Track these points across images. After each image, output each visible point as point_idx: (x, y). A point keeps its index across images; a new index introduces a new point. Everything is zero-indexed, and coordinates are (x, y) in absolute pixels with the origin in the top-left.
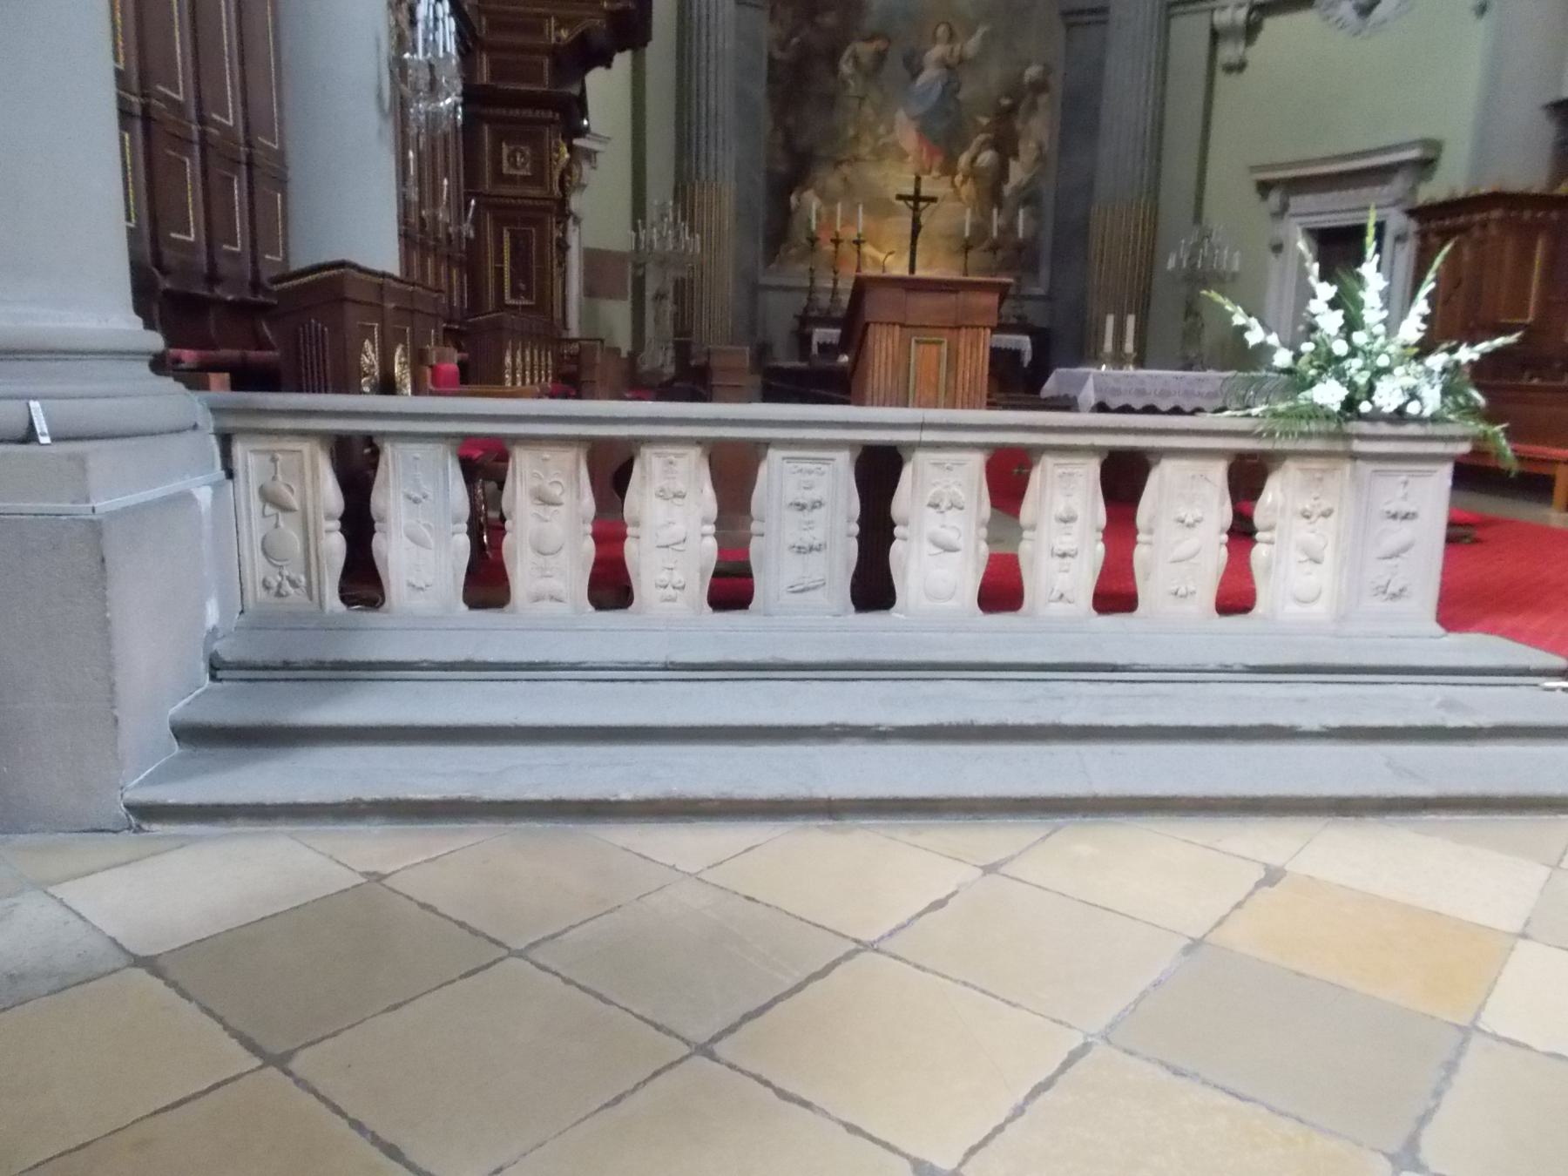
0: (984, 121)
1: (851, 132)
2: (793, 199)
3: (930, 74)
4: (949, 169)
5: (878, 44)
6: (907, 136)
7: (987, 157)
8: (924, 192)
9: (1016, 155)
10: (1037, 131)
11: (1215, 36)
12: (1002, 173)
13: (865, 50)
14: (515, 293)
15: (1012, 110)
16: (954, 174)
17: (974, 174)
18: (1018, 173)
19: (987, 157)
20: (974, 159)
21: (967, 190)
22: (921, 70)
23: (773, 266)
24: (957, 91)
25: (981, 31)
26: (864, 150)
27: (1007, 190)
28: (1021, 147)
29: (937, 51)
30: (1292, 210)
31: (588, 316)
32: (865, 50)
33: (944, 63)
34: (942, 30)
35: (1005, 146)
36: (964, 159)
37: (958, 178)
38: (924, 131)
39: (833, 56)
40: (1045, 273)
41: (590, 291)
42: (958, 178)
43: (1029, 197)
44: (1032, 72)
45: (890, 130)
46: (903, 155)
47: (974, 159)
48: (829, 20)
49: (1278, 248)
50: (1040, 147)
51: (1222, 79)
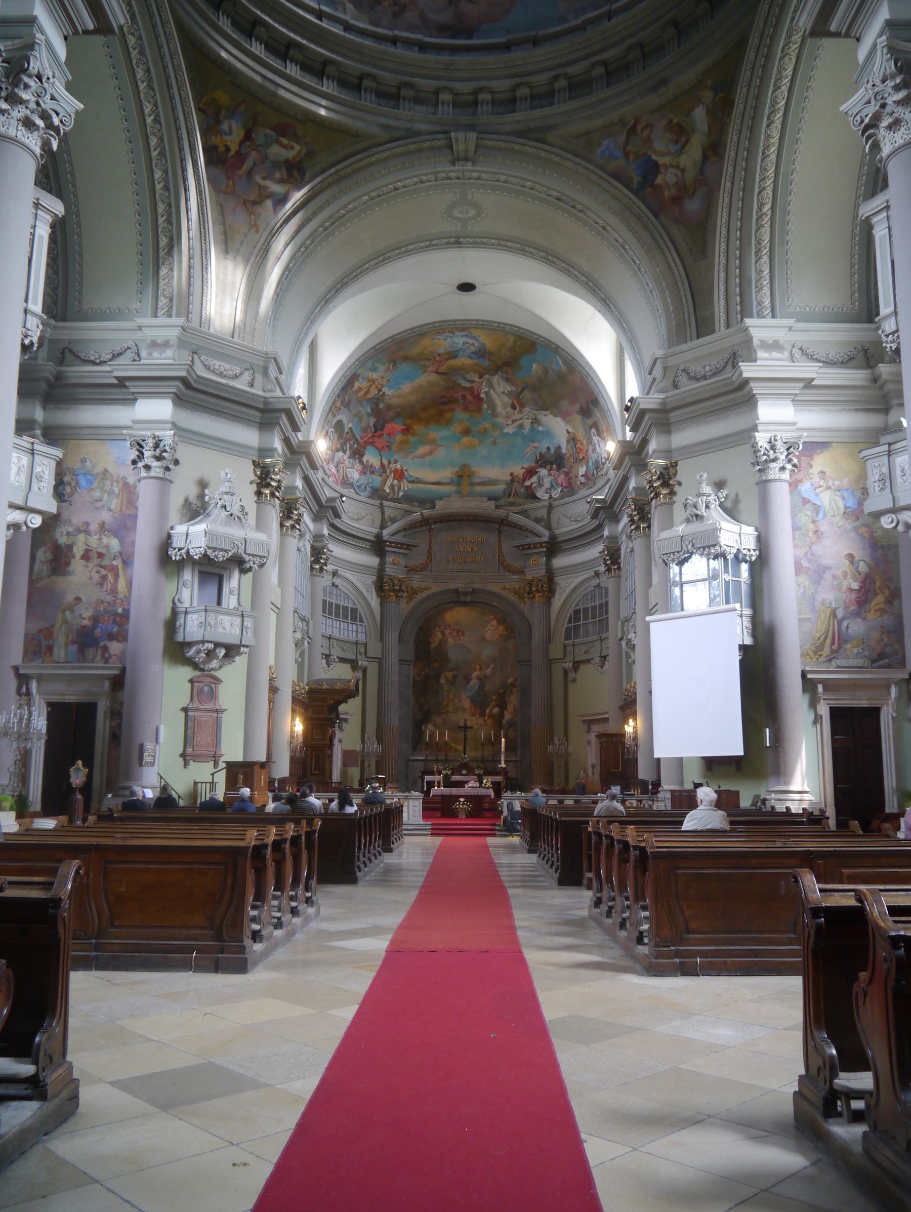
0: (494, 697)
1: (445, 702)
2: (423, 727)
3: (474, 682)
4: (482, 714)
5: (455, 672)
6: (467, 704)
7: (496, 710)
8: (468, 724)
9: (507, 710)
10: (513, 701)
11: (566, 672)
12: (502, 715)
13: (450, 675)
14: (315, 770)
15: (504, 694)
16: (485, 716)
17: (491, 716)
18: (507, 716)
19: (496, 710)
20: (491, 711)
21: (489, 722)
22: (470, 680)
23: (416, 753)
24: (484, 687)
25: (491, 666)
26: (450, 709)
27: (504, 721)
28: (508, 707)
29: (476, 674)
30: (592, 730)
31: (344, 774)
32: (450, 675)
33: (479, 678)
34: (477, 667)
35: (503, 706)
36: (488, 711)
37: (486, 717)
38: (472, 701)
39: (437, 677)
40: (519, 752)
41: (345, 765)
42: (486, 717)
43: (512, 724)
44: (510, 680)
45: (460, 701)
46: (465, 710)
47: (491, 711)
48: (436, 665)
49: (589, 743)
50: (515, 706)
51: (571, 686)
